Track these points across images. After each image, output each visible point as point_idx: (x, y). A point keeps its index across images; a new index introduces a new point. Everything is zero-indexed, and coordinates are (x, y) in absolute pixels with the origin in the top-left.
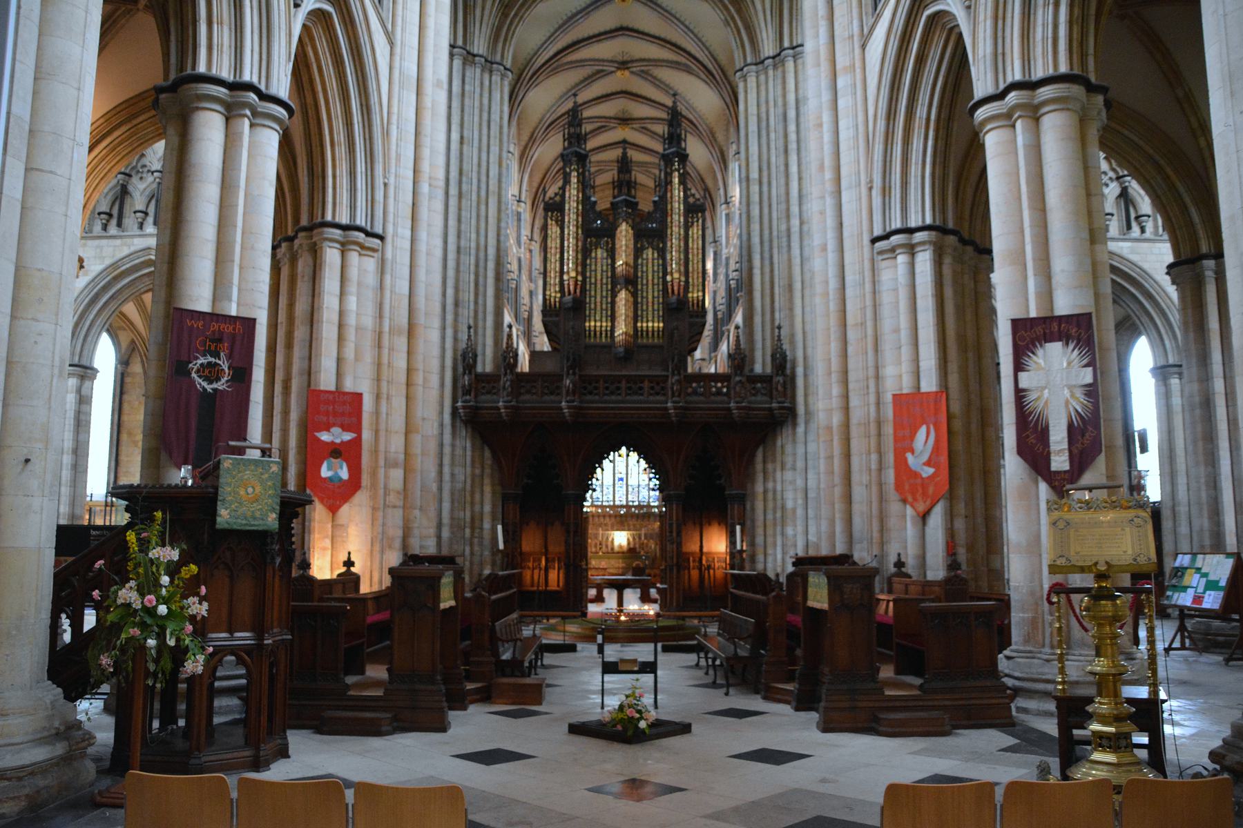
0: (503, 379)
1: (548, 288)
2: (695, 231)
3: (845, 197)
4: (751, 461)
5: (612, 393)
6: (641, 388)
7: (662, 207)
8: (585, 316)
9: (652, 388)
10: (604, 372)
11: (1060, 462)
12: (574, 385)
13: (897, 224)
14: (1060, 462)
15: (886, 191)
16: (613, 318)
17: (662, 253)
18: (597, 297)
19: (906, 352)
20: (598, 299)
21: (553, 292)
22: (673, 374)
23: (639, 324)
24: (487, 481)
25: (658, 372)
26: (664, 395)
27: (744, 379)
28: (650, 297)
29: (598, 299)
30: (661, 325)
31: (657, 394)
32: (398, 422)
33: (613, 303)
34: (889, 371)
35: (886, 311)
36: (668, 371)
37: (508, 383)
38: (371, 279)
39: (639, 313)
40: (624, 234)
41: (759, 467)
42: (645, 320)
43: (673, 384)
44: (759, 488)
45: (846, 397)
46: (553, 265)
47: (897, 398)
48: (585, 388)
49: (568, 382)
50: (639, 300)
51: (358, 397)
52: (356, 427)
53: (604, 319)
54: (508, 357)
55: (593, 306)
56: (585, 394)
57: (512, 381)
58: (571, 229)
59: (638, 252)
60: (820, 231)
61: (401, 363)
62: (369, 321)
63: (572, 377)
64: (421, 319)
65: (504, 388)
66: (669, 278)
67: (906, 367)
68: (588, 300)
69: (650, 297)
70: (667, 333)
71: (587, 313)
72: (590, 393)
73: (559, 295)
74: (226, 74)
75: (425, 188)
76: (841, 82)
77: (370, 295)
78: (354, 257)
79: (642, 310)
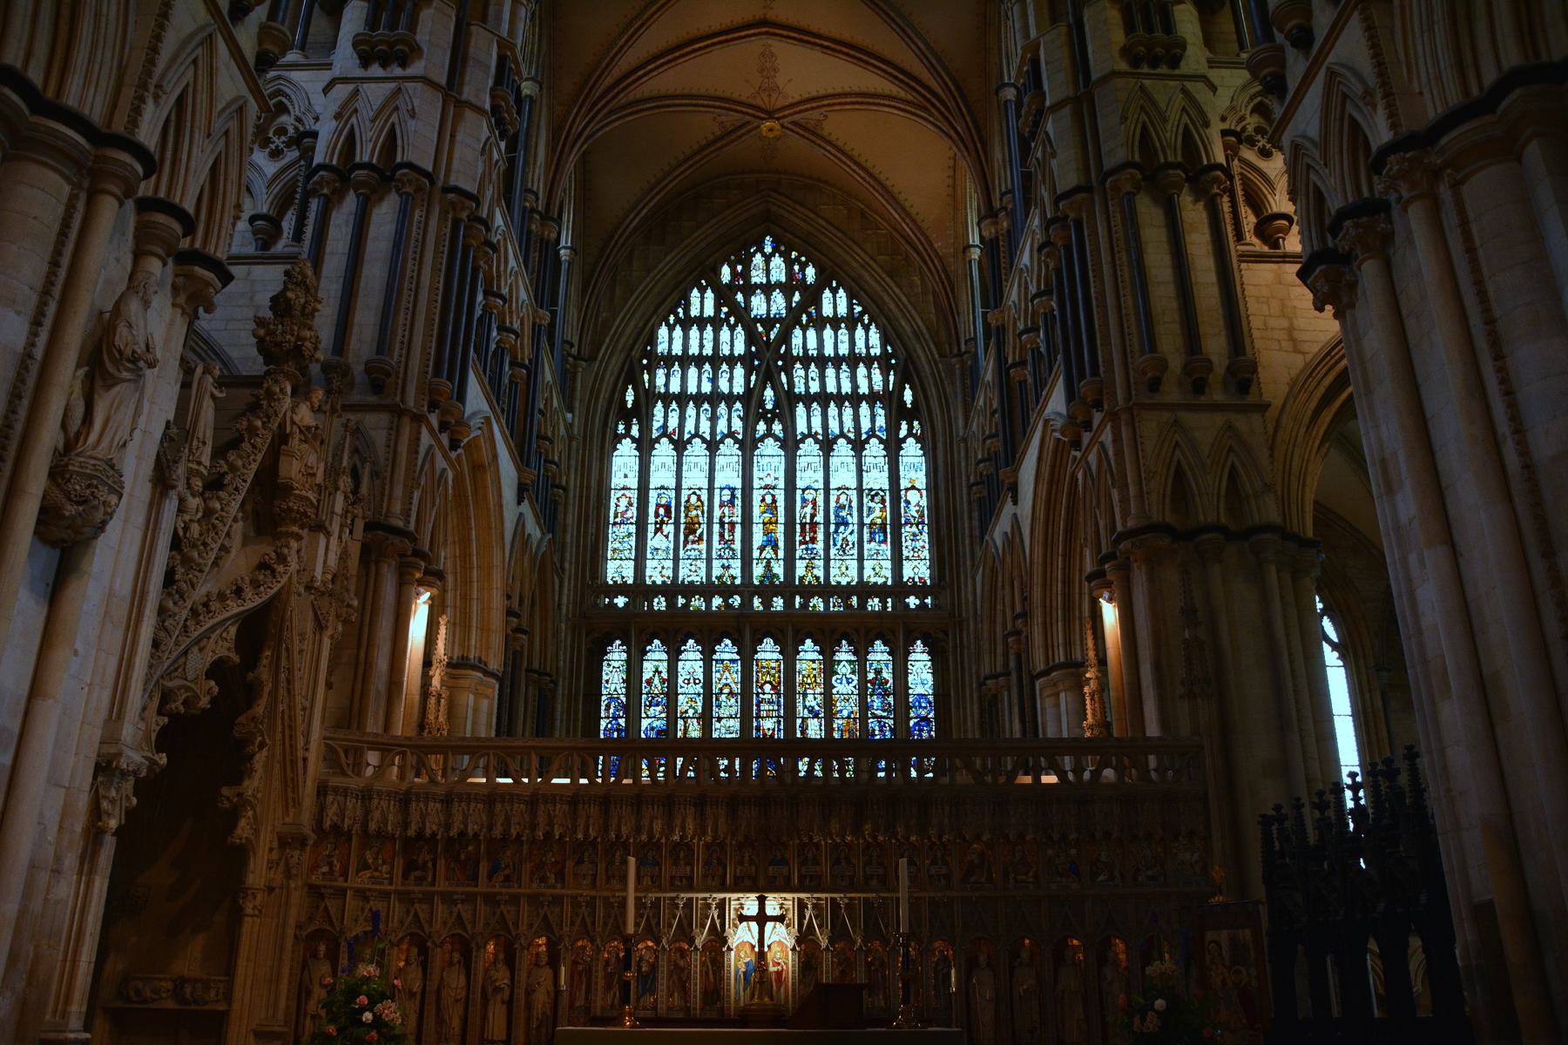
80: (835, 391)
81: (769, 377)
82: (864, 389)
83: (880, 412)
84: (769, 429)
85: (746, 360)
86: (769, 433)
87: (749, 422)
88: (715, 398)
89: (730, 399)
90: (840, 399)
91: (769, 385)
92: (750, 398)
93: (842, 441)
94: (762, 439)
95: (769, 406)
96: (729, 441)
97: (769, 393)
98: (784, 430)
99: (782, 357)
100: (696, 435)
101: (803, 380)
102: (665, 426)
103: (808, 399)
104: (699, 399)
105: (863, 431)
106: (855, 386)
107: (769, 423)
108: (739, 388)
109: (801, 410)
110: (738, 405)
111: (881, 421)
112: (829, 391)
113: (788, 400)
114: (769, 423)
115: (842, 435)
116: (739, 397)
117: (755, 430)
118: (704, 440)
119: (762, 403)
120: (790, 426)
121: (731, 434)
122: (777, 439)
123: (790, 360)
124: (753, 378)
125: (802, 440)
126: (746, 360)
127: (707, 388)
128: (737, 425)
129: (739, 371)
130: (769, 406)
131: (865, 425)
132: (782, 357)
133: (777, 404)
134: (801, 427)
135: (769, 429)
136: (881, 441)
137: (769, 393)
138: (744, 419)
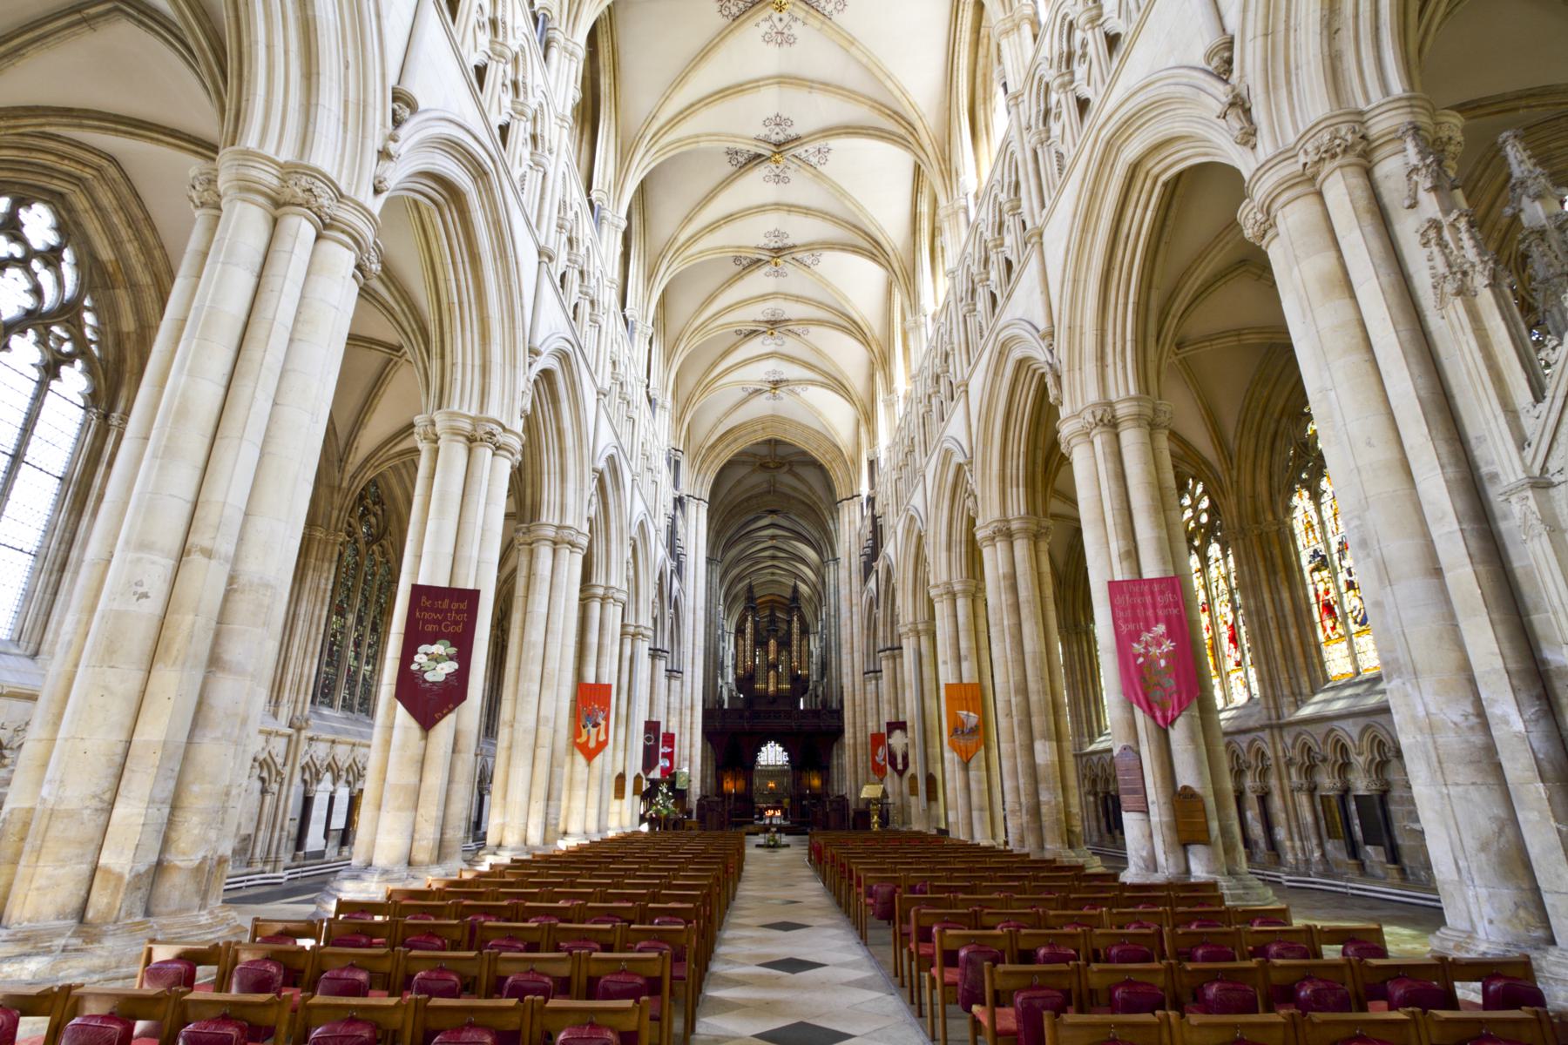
2: (805, 643)
3: (856, 655)
4: (832, 749)
7: (789, 633)
10: (763, 708)
11: (900, 767)
13: (889, 645)
14: (900, 767)
15: (868, 655)
16: (767, 683)
17: (790, 653)
18: (760, 674)
19: (875, 718)
21: (741, 672)
25: (788, 708)
32: (687, 743)
33: (768, 677)
34: (870, 724)
35: (868, 701)
38: (678, 689)
40: (772, 642)
41: (835, 752)
44: (835, 762)
45: (855, 733)
46: (741, 658)
47: (872, 735)
51: (673, 735)
52: (672, 746)
54: (720, 702)
58: (748, 642)
59: (778, 652)
60: (846, 669)
61: (688, 720)
62: (677, 705)
64: (695, 702)
67: (874, 723)
70: (793, 690)
74: (603, 583)
75: (697, 651)
76: (854, 609)
77: (678, 696)
78: (673, 681)
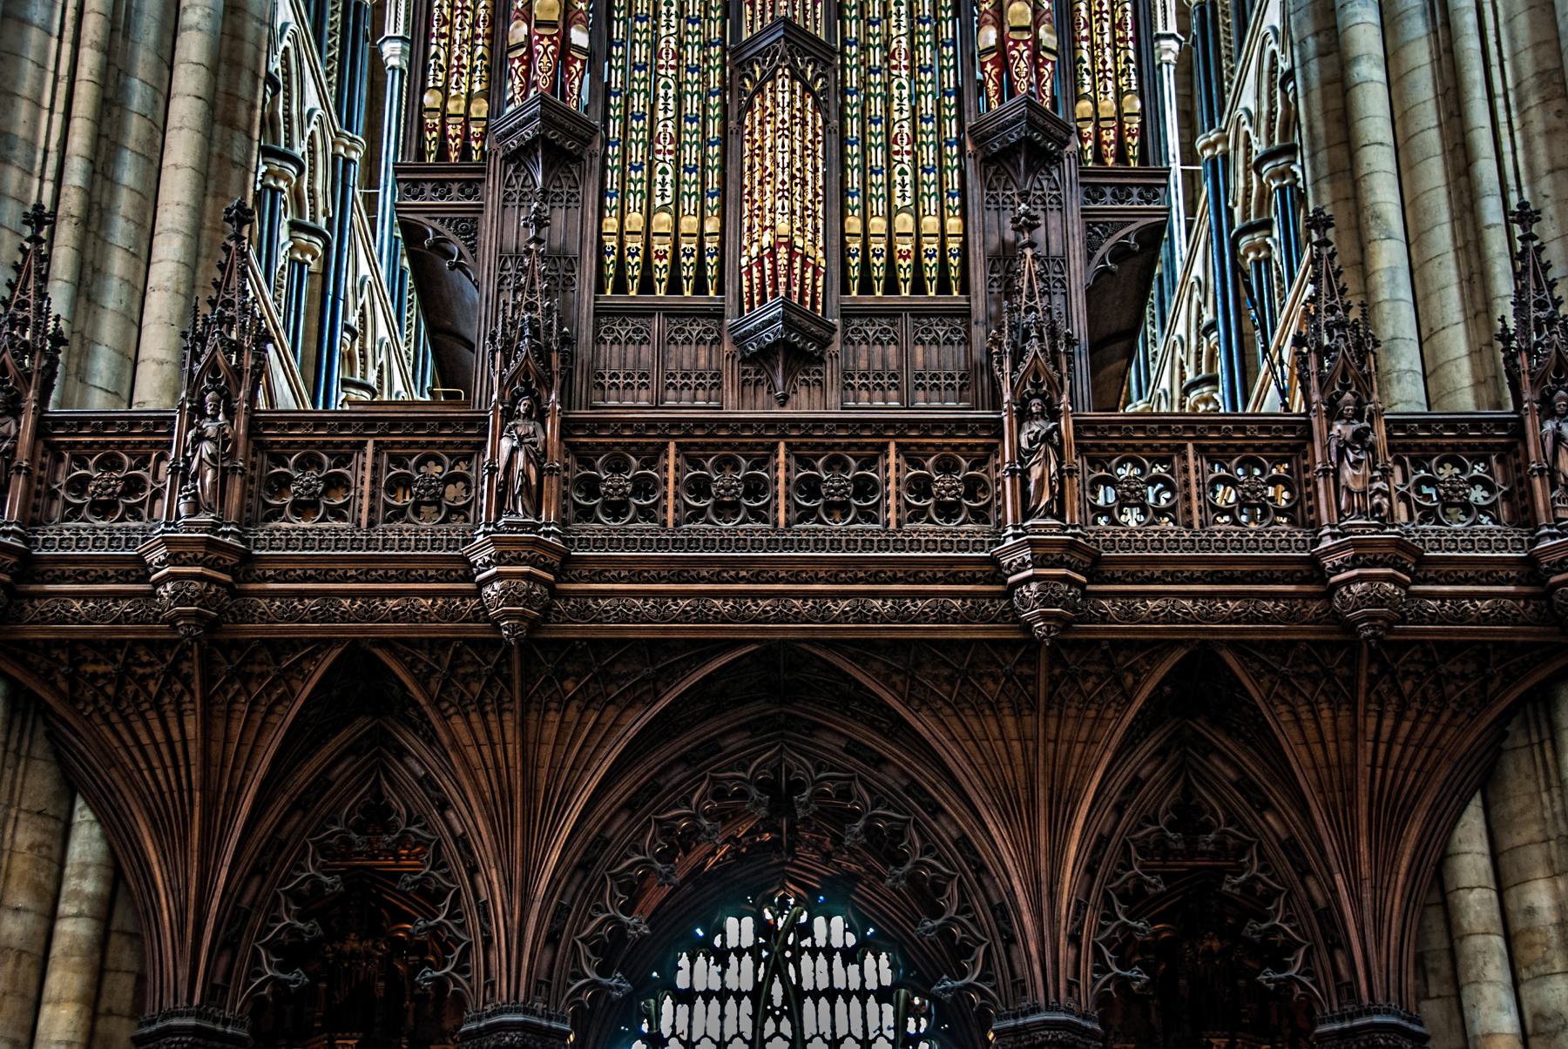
0: (181, 433)
1: (435, 78)
5: (725, 509)
6: (865, 487)
8: (603, 193)
9: (921, 487)
12: (538, 458)
20: (665, 128)
22: (1023, 416)
23: (854, 224)
24: (64, 980)
26: (979, 515)
27: (1380, 435)
28: (901, 115)
29: (665, 128)
30: (954, 224)
31: (948, 511)
36: (996, 404)
37: (207, 448)
39: (854, 179)
41: (1477, 905)
42: (879, 206)
43: (1022, 455)
48: (590, 487)
49: (506, 444)
50: (853, 128)
53: (690, 204)
55: (637, 153)
56: (586, 514)
57: (222, 440)
63: (524, 427)
65: (183, 474)
66: (989, 36)
68: (615, 128)
69: (901, 115)
71: (613, 179)
72: (616, 510)
73: (480, 108)
79: (866, 170)
80: (843, 987)
81: (777, 968)
82: (871, 984)
83: (888, 1009)
84: (778, 1028)
85: (754, 951)
86: (778, 1033)
87: (757, 1020)
88: (723, 995)
89: (739, 996)
90: (847, 994)
91: (777, 979)
92: (759, 994)
93: (849, 1040)
94: (770, 1039)
95: (777, 1002)
96: (738, 1040)
97: (777, 990)
98: (793, 1029)
99: (790, 948)
100: (705, 1035)
101: (812, 972)
102: (674, 1027)
103: (816, 995)
104: (707, 995)
105: (871, 1030)
106: (863, 981)
107: (777, 1020)
108: (747, 985)
109: (808, 1002)
110: (746, 1002)
111: (889, 1020)
112: (836, 986)
113: (796, 995)
114: (777, 1020)
115: (850, 1034)
116: (747, 993)
117: (763, 1029)
118: (713, 1041)
119: (770, 999)
120: (798, 1027)
121: (740, 1034)
122: (785, 1038)
123: (798, 952)
124: (761, 971)
125: (810, 1040)
126: (754, 951)
127: (716, 985)
128: (747, 1028)
129: (747, 960)
130: (777, 1002)
131: (873, 1024)
132: (790, 948)
133: (785, 1000)
134: (809, 1030)
135: (778, 1028)
136: (889, 1041)
137: (777, 990)
138: (753, 1017)
